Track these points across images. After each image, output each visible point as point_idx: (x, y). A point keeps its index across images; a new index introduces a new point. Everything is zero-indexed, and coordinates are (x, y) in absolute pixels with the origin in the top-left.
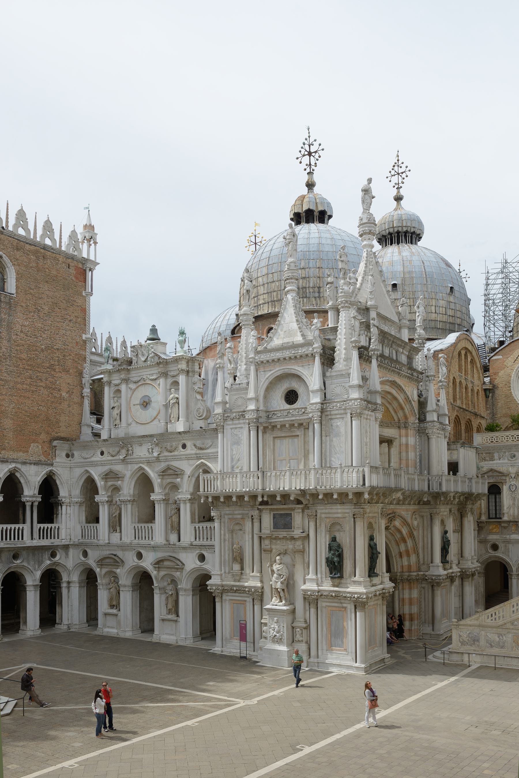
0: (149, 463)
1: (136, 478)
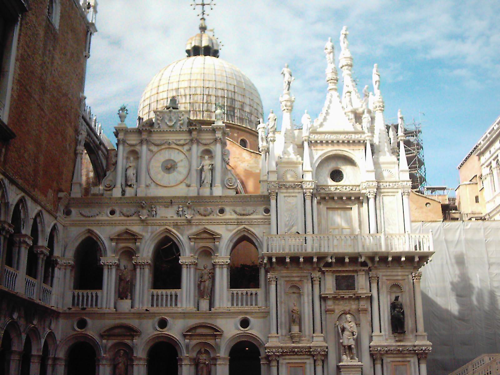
0: (176, 225)
1: (156, 241)
